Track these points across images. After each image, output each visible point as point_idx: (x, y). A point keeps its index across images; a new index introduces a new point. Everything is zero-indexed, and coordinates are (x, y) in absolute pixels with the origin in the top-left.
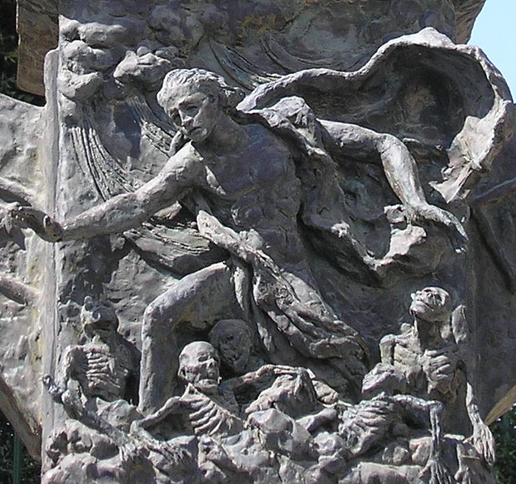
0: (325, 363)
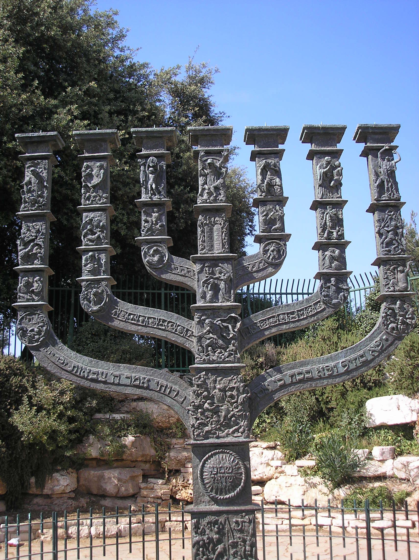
0: (223, 348)
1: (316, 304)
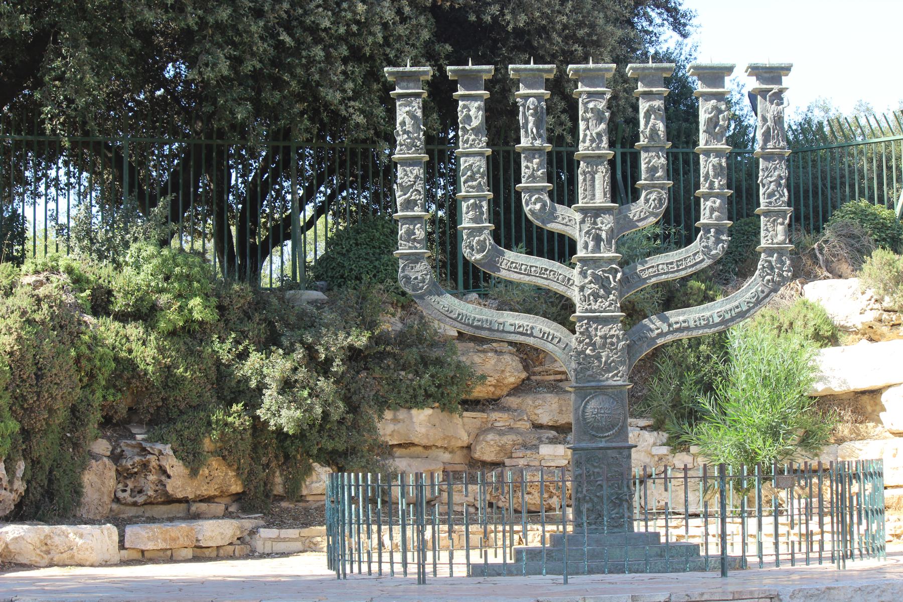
1: (695, 255)
